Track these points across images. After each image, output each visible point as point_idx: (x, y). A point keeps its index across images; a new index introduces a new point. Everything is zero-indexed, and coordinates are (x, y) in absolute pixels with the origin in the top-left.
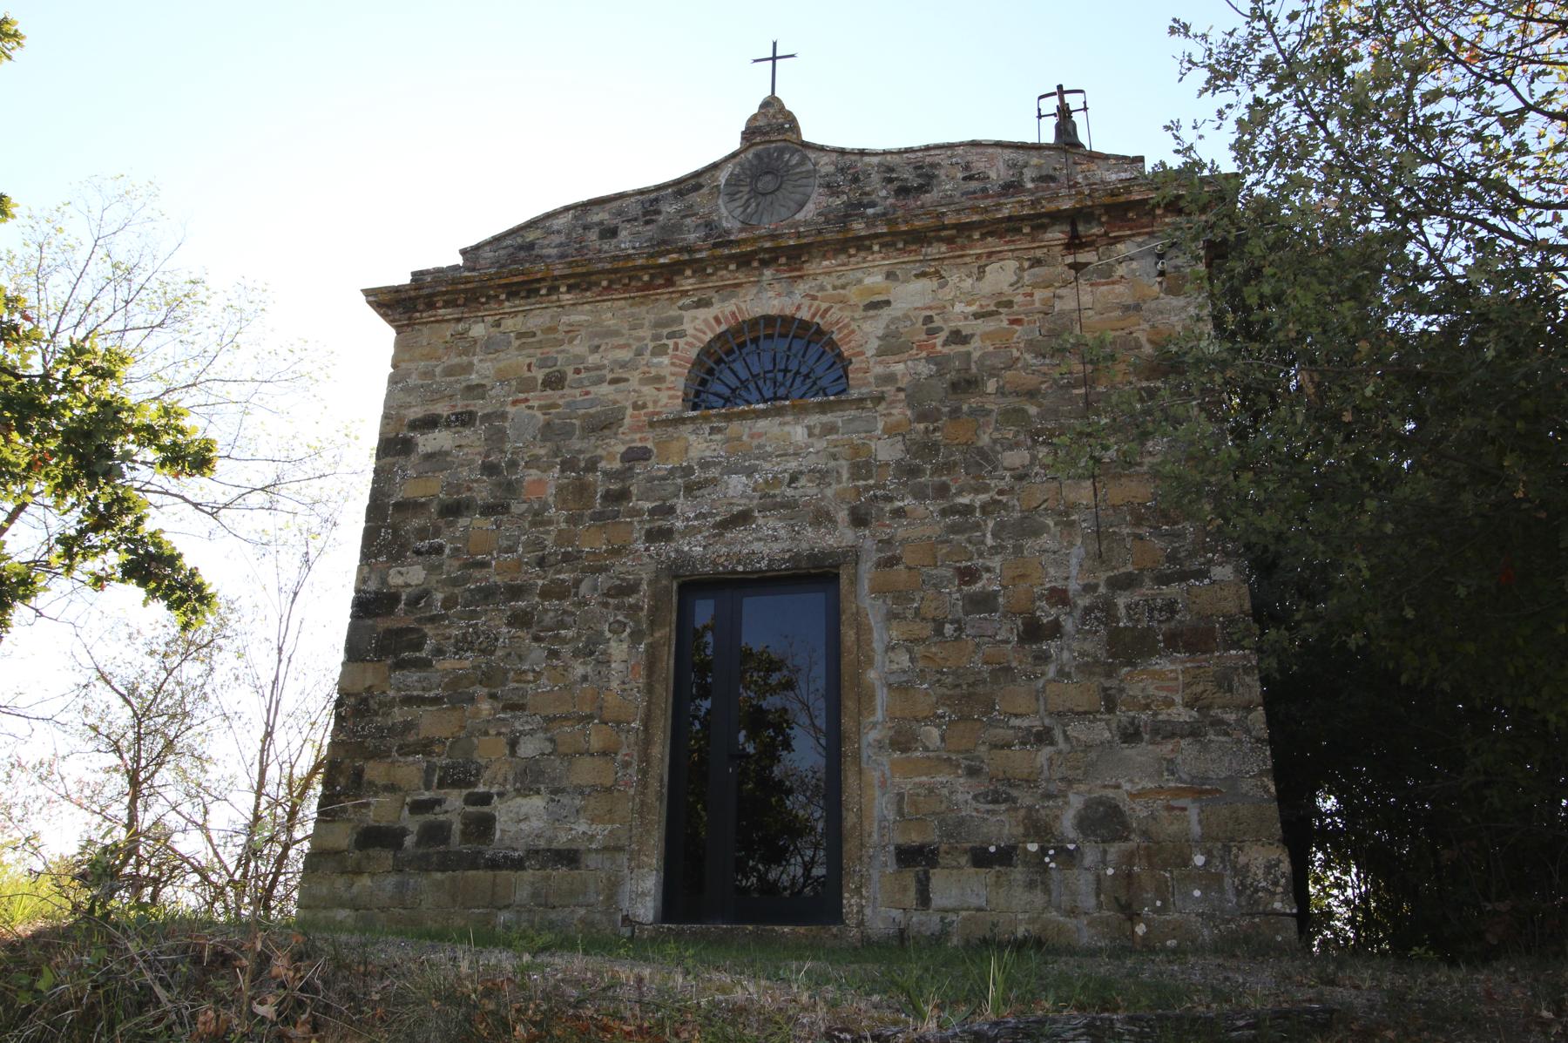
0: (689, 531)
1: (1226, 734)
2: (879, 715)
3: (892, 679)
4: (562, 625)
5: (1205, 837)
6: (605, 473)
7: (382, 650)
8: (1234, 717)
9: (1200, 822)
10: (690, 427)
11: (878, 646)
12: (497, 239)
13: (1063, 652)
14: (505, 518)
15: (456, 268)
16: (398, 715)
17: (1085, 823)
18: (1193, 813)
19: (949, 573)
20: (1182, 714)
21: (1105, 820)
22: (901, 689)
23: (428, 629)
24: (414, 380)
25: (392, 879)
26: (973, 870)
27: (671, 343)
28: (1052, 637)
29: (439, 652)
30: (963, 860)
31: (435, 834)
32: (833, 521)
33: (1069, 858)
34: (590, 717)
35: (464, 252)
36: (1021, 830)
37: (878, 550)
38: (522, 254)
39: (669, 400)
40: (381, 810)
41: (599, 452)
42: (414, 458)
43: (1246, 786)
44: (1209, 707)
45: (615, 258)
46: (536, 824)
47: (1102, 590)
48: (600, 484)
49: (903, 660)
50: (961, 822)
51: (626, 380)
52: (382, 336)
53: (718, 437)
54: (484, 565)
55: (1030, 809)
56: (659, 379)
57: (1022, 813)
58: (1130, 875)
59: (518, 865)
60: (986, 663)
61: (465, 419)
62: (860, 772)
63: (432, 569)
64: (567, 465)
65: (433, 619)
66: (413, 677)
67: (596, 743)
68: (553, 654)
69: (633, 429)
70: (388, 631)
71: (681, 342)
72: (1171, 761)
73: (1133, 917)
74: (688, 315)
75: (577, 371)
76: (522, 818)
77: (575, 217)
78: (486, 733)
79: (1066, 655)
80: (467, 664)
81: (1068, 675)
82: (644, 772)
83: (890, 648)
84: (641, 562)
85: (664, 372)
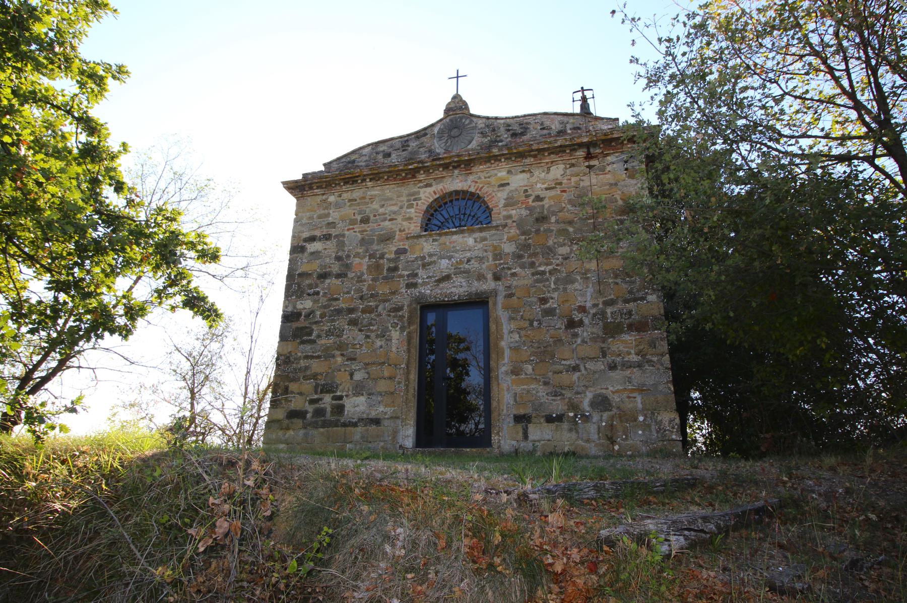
1: (653, 366)
2: (506, 361)
3: (511, 345)
4: (371, 324)
6: (388, 259)
7: (295, 336)
10: (424, 239)
11: (505, 331)
12: (339, 159)
13: (584, 333)
15: (321, 172)
16: (303, 363)
17: (593, 404)
18: (639, 399)
19: (535, 300)
20: (634, 358)
21: (602, 403)
22: (515, 349)
23: (314, 327)
24: (304, 221)
25: (302, 432)
27: (415, 203)
29: (319, 336)
30: (542, 420)
31: (319, 412)
32: (486, 279)
33: (586, 419)
34: (384, 363)
35: (325, 165)
39: (415, 227)
40: (297, 403)
41: (385, 250)
42: (306, 254)
43: (661, 388)
44: (646, 355)
45: (390, 166)
46: (362, 408)
47: (601, 306)
50: (541, 404)
52: (290, 202)
55: (570, 398)
56: (410, 219)
58: (612, 425)
59: (355, 425)
61: (327, 237)
62: (498, 384)
63: (315, 302)
64: (371, 256)
65: (316, 323)
66: (308, 347)
67: (386, 374)
68: (368, 337)
69: (400, 240)
70: (297, 328)
71: (419, 202)
73: (613, 442)
74: (422, 190)
75: (375, 216)
76: (356, 406)
77: (373, 149)
79: (585, 334)
81: (586, 342)
82: (407, 386)
84: (404, 297)
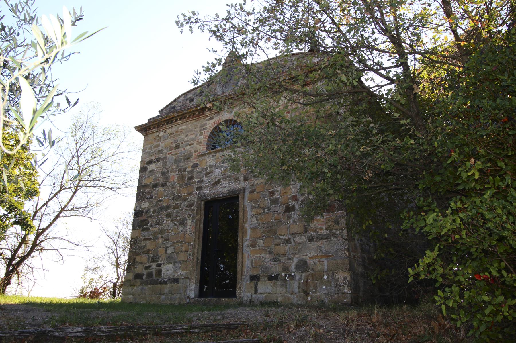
0: (206, 187)
1: (336, 238)
2: (248, 237)
3: (252, 226)
4: (177, 216)
5: (329, 270)
6: (188, 172)
7: (140, 226)
8: (338, 232)
9: (327, 265)
10: (207, 156)
11: (249, 217)
12: (167, 106)
13: (295, 215)
14: (166, 187)
15: (158, 116)
16: (143, 243)
17: (298, 267)
18: (326, 263)
19: (267, 193)
20: (324, 232)
21: (303, 266)
22: (254, 229)
23: (149, 220)
24: (148, 150)
25: (140, 287)
26: (268, 282)
27: (203, 131)
28: (292, 211)
29: (151, 226)
30: (266, 279)
31: (150, 275)
32: (239, 180)
33: (292, 277)
34: (183, 241)
35: (159, 111)
36: (281, 269)
37: (250, 188)
38: (172, 110)
39: (202, 149)
40: (139, 269)
41: (187, 166)
42: (147, 172)
43: (340, 254)
44: (332, 230)
45: (188, 109)
46: (170, 272)
47: (306, 195)
48: (187, 175)
49: (255, 220)
50: (267, 267)
51: (193, 144)
52: (140, 137)
53: (213, 158)
54: (161, 201)
55: (284, 263)
56: (201, 143)
57: (282, 264)
58: (307, 282)
59: (166, 283)
60: (275, 220)
61: (158, 160)
62: (242, 254)
63: (150, 203)
64: (180, 171)
65: (150, 217)
66: (145, 233)
67: (184, 249)
68: (175, 224)
69: (195, 158)
70: (141, 221)
71: (206, 131)
72: (321, 247)
73: (307, 294)
74: (208, 122)
75: (182, 143)
76: (168, 270)
77: (184, 97)
78: (160, 247)
79: (295, 216)
80: (157, 228)
81: (296, 222)
82: (193, 256)
83: (252, 217)
84: (194, 199)
85: (202, 141)
